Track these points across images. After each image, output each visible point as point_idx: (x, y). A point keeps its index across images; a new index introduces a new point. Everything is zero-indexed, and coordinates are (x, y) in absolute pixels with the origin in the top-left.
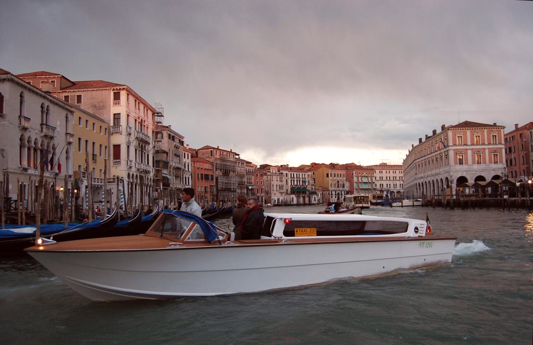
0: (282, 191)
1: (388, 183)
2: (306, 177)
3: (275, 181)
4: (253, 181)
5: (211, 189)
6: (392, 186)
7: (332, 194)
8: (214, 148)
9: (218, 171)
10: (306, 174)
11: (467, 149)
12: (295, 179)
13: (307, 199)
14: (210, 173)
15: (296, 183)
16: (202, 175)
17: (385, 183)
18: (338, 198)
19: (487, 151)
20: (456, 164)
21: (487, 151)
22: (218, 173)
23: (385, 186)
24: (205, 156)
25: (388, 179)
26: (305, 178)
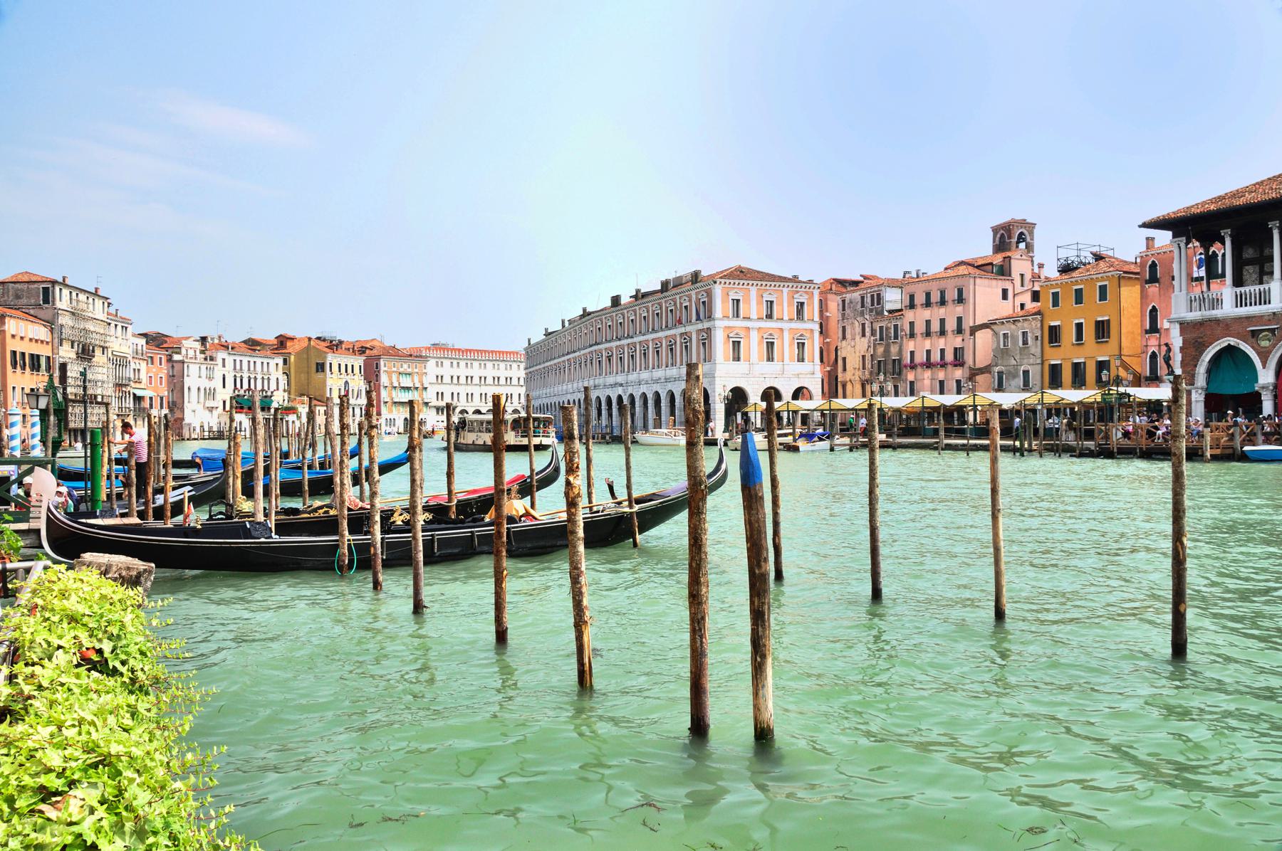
0: (210, 403)
1: (456, 389)
3: (194, 378)
4: (143, 376)
6: (463, 397)
8: (54, 283)
9: (66, 346)
10: (272, 363)
11: (748, 328)
14: (44, 351)
15: (246, 386)
16: (23, 354)
17: (447, 390)
20: (726, 359)
21: (786, 335)
22: (67, 353)
24: (24, 301)
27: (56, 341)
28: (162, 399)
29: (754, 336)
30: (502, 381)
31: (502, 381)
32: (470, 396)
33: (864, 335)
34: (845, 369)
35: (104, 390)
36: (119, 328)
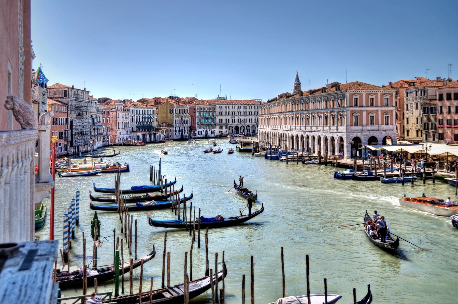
2: (151, 113)
5: (65, 134)
6: (231, 121)
7: (176, 131)
8: (69, 88)
9: (73, 112)
11: (362, 111)
12: (141, 116)
13: (153, 137)
15: (141, 120)
17: (224, 118)
18: (182, 134)
19: (380, 113)
21: (380, 113)
23: (224, 121)
25: (227, 114)
26: (150, 114)
27: (69, 112)
28: (108, 128)
29: (364, 114)
30: (248, 113)
31: (248, 113)
32: (234, 121)
33: (417, 108)
34: (408, 123)
35: (87, 129)
36: (93, 103)
